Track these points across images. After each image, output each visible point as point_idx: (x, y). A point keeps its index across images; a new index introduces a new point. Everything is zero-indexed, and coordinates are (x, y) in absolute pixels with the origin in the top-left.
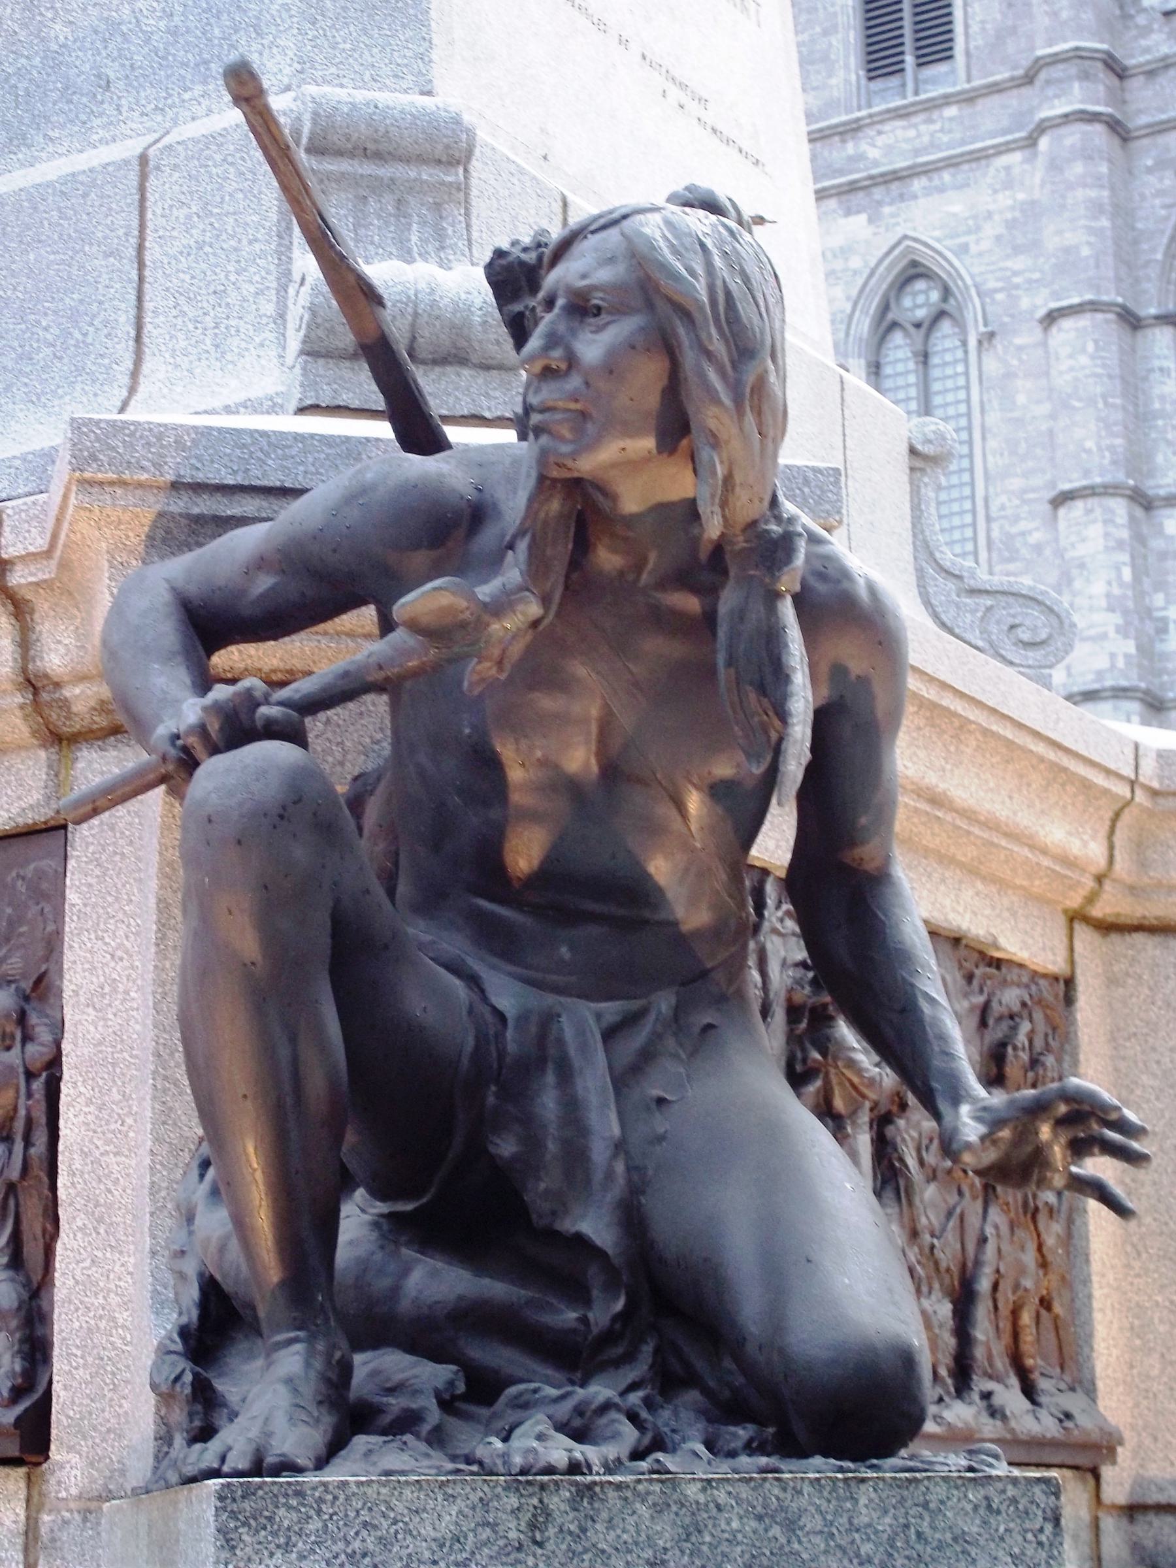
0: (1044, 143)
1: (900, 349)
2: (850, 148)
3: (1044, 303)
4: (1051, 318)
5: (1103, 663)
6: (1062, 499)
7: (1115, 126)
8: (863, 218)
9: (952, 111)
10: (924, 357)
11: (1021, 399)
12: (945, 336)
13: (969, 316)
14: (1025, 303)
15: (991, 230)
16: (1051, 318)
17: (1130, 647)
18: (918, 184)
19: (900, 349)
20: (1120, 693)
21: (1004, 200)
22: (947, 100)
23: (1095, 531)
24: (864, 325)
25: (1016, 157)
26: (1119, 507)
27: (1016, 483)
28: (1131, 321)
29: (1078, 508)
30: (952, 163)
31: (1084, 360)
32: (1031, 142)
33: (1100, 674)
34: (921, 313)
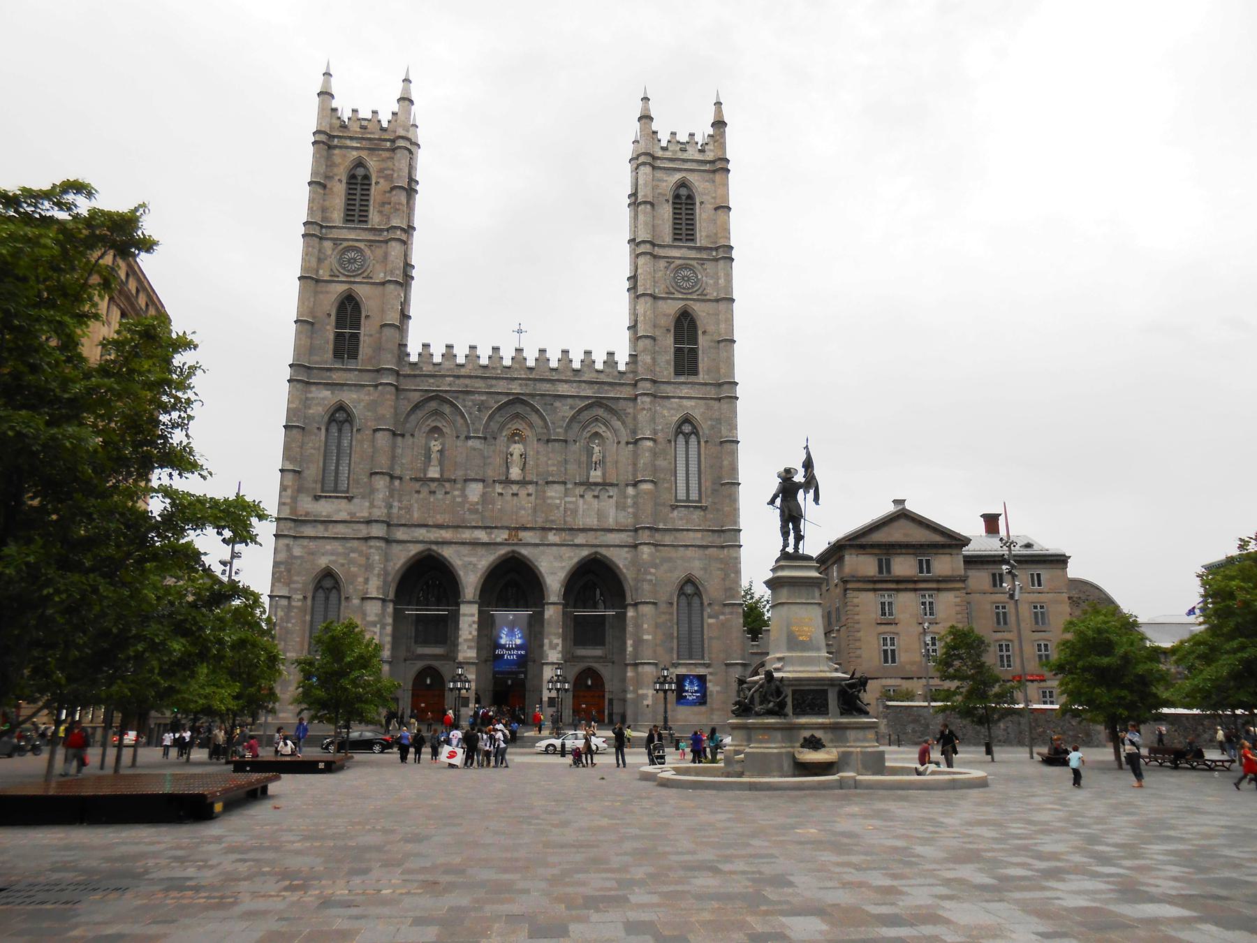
0: (380, 388)
2: (328, 374)
3: (373, 425)
4: (376, 431)
5: (379, 514)
6: (372, 474)
7: (397, 388)
8: (330, 392)
9: (357, 373)
11: (365, 446)
12: (346, 427)
13: (354, 423)
14: (369, 424)
15: (362, 404)
16: (376, 431)
17: (386, 511)
18: (345, 388)
20: (383, 522)
21: (367, 397)
22: (356, 370)
23: (382, 483)
24: (326, 418)
25: (371, 388)
26: (388, 478)
27: (361, 466)
28: (394, 434)
29: (378, 477)
30: (355, 385)
31: (384, 442)
32: (376, 386)
33: (379, 517)
34: (341, 419)
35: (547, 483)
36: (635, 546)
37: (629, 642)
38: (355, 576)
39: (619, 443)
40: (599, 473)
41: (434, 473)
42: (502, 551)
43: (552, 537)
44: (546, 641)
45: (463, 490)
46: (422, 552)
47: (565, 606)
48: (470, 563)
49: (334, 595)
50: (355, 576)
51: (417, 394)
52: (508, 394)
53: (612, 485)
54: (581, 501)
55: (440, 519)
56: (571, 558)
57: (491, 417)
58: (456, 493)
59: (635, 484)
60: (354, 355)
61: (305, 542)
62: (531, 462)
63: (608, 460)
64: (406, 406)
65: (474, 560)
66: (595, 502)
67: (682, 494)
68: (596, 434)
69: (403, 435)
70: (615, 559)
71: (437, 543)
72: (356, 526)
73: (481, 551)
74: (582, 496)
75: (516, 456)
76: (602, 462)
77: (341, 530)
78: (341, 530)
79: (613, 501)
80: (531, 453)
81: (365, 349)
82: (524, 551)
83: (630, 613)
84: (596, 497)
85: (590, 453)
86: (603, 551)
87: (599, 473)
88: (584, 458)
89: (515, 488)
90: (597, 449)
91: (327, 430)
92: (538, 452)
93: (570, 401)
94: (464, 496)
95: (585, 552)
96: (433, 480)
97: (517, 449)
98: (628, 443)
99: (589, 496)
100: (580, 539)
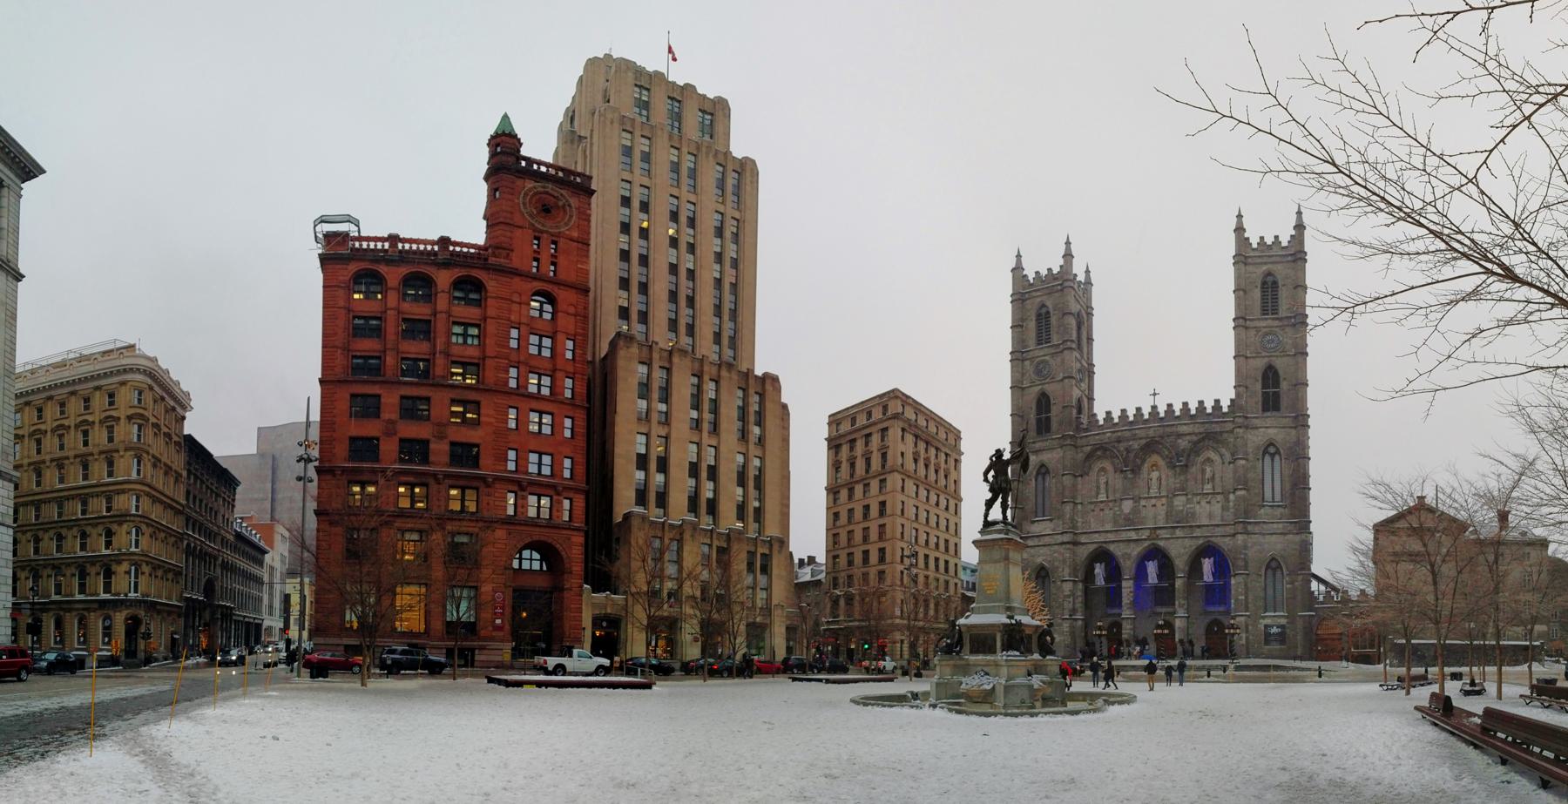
1: (1040, 478)
3: (1061, 472)
4: (1063, 475)
10: (1044, 479)
19: (1040, 478)
35: (1175, 495)
36: (1234, 535)
37: (1233, 601)
38: (1058, 568)
39: (1223, 463)
40: (1210, 486)
41: (1102, 497)
42: (1146, 544)
43: (1178, 533)
44: (1177, 603)
45: (1120, 506)
46: (1096, 549)
47: (1188, 579)
48: (1126, 553)
49: (1047, 580)
50: (1058, 568)
51: (1089, 448)
52: (1146, 438)
53: (1218, 493)
54: (1198, 506)
55: (1108, 527)
56: (1191, 546)
57: (1136, 457)
58: (1117, 509)
59: (1234, 493)
60: (1048, 430)
61: (1028, 550)
62: (1163, 482)
63: (1217, 476)
64: (1081, 456)
65: (1129, 551)
66: (1208, 506)
67: (1268, 495)
68: (1209, 459)
69: (1081, 476)
70: (1221, 544)
71: (1105, 542)
72: (1056, 537)
73: (1132, 545)
74: (1199, 503)
75: (1154, 481)
76: (1213, 478)
77: (1047, 540)
78: (1047, 540)
79: (1220, 505)
80: (1163, 477)
81: (1054, 425)
82: (1161, 543)
83: (1233, 581)
84: (1209, 502)
85: (1203, 471)
86: (1213, 539)
87: (1210, 486)
88: (1200, 476)
89: (1153, 501)
90: (1208, 469)
91: (1036, 480)
92: (1167, 476)
93: (1188, 438)
94: (1121, 510)
95: (1201, 541)
96: (1102, 502)
97: (1155, 475)
98: (1230, 463)
99: (1203, 503)
100: (1198, 533)
